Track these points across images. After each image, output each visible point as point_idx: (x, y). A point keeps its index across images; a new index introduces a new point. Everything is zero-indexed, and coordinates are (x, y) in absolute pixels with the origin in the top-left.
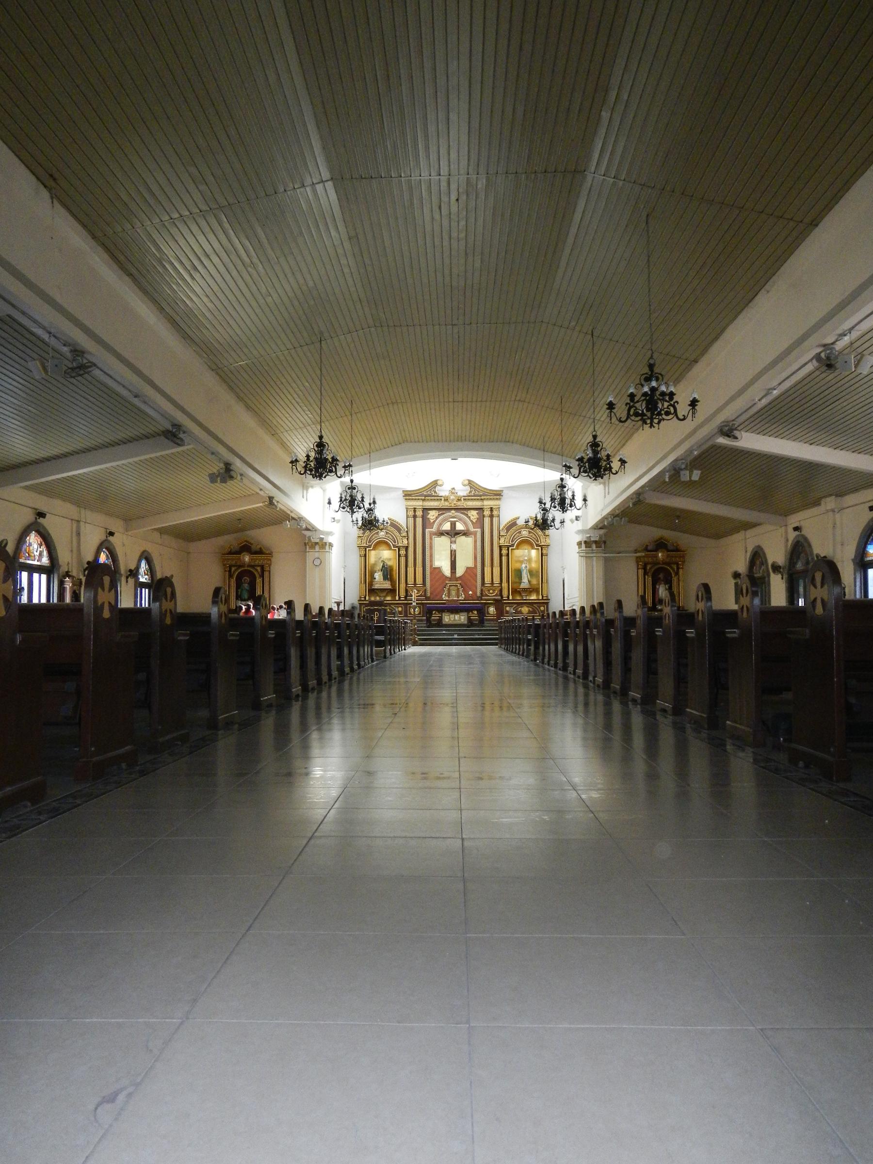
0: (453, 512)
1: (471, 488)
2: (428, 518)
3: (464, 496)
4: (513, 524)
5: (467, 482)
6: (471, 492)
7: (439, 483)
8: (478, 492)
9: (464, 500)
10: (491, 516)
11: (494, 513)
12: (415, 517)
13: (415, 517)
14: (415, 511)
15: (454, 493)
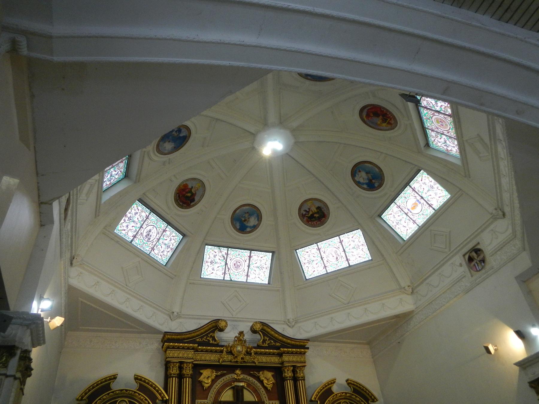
0: (238, 372)
1: (264, 335)
2: (202, 381)
3: (255, 348)
4: (327, 392)
5: (258, 327)
6: (264, 341)
7: (222, 324)
8: (275, 342)
9: (256, 353)
10: (295, 380)
11: (298, 375)
12: (181, 377)
13: (181, 377)
14: (181, 368)
15: (241, 340)
